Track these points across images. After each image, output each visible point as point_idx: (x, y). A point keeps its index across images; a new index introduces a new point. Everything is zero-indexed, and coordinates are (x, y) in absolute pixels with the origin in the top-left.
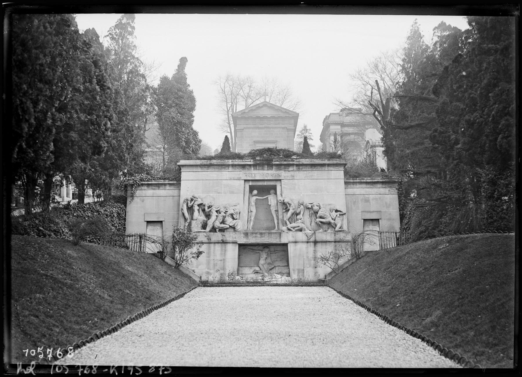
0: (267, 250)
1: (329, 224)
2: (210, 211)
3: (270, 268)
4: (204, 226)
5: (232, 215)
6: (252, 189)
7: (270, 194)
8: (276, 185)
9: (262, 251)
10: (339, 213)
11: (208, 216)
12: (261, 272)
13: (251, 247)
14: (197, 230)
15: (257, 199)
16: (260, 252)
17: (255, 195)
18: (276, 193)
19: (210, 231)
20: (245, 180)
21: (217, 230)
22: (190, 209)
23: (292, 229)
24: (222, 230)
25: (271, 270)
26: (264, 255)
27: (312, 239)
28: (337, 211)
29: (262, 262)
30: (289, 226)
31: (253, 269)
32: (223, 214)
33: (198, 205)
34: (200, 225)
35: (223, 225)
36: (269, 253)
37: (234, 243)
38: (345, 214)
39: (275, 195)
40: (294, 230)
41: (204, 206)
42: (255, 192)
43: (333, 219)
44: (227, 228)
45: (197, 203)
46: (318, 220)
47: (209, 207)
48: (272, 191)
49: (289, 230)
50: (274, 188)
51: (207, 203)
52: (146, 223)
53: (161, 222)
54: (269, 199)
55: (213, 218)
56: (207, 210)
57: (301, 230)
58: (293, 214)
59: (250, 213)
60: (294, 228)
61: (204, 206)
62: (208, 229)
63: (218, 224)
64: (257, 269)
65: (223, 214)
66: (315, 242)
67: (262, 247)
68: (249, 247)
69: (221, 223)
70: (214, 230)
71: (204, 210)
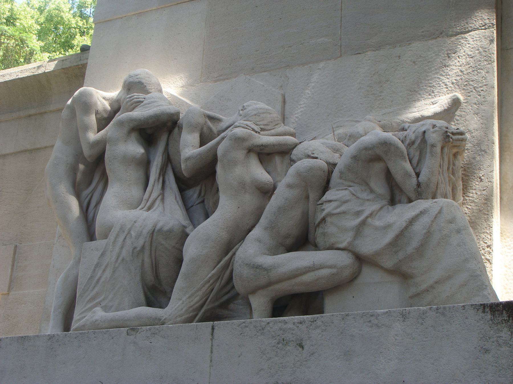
24: (300, 301)
44: (341, 284)
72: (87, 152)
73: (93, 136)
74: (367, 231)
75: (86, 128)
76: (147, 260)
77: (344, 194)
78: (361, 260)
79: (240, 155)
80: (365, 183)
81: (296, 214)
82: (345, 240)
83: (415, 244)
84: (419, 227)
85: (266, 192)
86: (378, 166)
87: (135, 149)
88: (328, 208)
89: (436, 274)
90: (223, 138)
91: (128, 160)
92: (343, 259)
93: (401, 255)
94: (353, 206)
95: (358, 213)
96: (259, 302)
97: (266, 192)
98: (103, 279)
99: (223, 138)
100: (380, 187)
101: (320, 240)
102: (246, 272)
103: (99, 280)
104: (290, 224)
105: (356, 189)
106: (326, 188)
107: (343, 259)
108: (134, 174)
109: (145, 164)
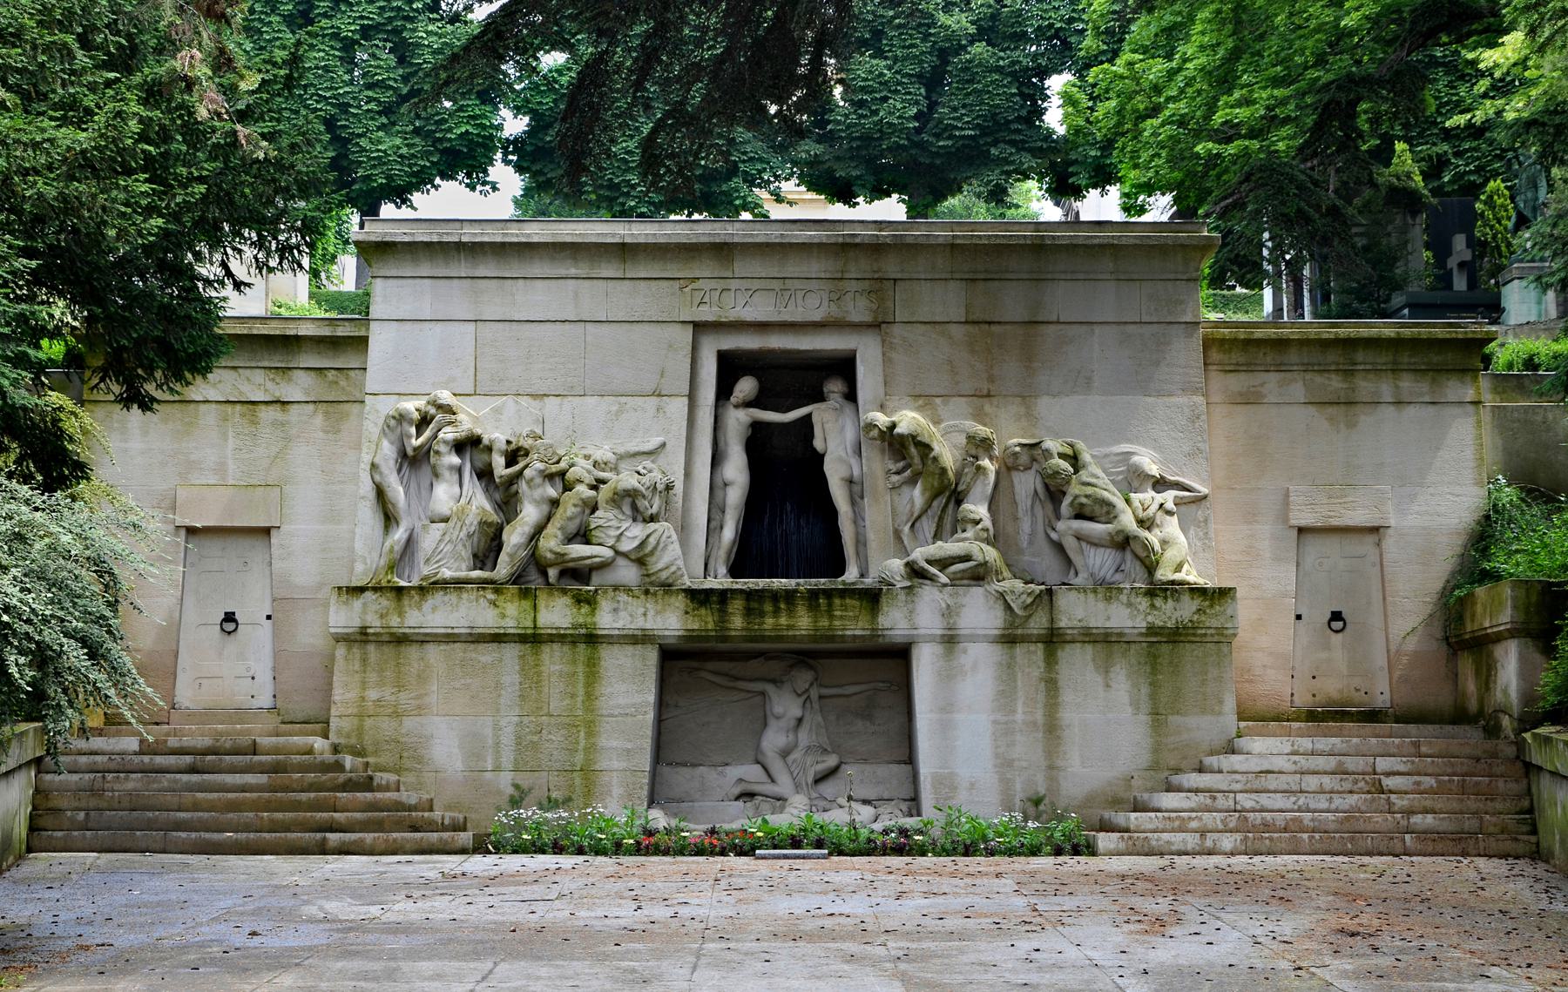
0: (803, 678)
1: (1123, 542)
2: (520, 474)
3: (820, 767)
4: (488, 547)
5: (631, 495)
6: (730, 367)
7: (819, 397)
9: (774, 681)
10: (1169, 497)
11: (507, 500)
12: (769, 788)
13: (726, 666)
14: (447, 573)
15: (756, 426)
16: (770, 688)
17: (748, 404)
18: (851, 396)
19: (517, 578)
20: (699, 327)
21: (553, 573)
22: (414, 461)
23: (933, 570)
24: (577, 574)
25: (817, 781)
26: (786, 705)
27: (1038, 624)
28: (1160, 484)
29: (774, 739)
30: (919, 554)
31: (734, 772)
32: (582, 490)
33: (459, 447)
34: (466, 554)
35: (578, 550)
36: (814, 693)
37: (640, 639)
38: (1205, 497)
40: (944, 579)
41: (489, 449)
42: (746, 387)
43: (1141, 522)
44: (604, 565)
45: (448, 434)
46: (1067, 527)
47: (513, 457)
48: (835, 387)
49: (916, 573)
50: (844, 367)
51: (497, 435)
52: (183, 533)
53: (266, 531)
54: (815, 419)
55: (530, 513)
56: (500, 468)
57: (979, 575)
59: (719, 493)
60: (943, 563)
61: (489, 449)
62: (503, 569)
63: (550, 543)
64: (752, 772)
65: (582, 490)
66: (1053, 640)
68: (711, 665)
69: (570, 540)
70: (536, 572)
71: (485, 474)
72: (410, 452)
73: (416, 442)
75: (410, 437)
77: (610, 515)
78: (617, 553)
79: (538, 480)
80: (619, 508)
81: (577, 521)
82: (611, 542)
83: (649, 548)
84: (652, 540)
85: (555, 503)
86: (628, 500)
87: (455, 460)
88: (601, 522)
89: (660, 565)
91: (451, 468)
92: (609, 553)
94: (614, 523)
96: (553, 573)
97: (555, 503)
100: (627, 509)
101: (594, 540)
102: (549, 555)
104: (573, 527)
105: (616, 512)
106: (594, 509)
107: (609, 553)
109: (460, 470)
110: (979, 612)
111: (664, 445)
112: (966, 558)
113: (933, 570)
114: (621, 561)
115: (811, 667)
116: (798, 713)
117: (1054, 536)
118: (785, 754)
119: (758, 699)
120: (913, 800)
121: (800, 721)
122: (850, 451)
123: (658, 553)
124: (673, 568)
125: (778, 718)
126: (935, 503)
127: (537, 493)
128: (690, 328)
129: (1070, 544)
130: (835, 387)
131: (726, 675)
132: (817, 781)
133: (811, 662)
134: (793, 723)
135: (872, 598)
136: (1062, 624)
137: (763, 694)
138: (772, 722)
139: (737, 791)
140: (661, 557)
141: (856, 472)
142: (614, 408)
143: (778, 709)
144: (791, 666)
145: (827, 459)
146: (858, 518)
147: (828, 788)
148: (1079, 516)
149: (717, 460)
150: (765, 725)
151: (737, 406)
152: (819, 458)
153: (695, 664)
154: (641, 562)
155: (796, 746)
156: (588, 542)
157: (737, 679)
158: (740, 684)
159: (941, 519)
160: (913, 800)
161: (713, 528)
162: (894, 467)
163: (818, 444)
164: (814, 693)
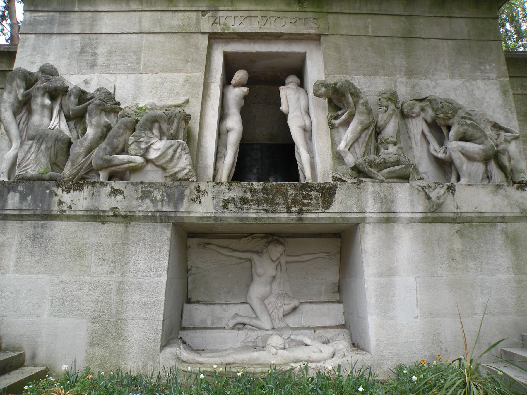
0: (276, 251)
3: (288, 308)
8: (305, 54)
9: (257, 252)
16: (255, 257)
18: (302, 85)
25: (284, 316)
26: (265, 267)
29: (257, 290)
31: (233, 309)
39: (302, 91)
42: (240, 75)
46: (454, 145)
48: (292, 79)
58: (365, 129)
59: (223, 137)
67: (264, 241)
74: (151, 150)
76: (52, 152)
87: (48, 102)
90: (90, 104)
92: (139, 160)
93: (163, 161)
95: (147, 143)
98: (31, 158)
99: (90, 104)
103: (29, 158)
108: (47, 112)
110: (406, 200)
111: (188, 101)
112: (397, 163)
113: (374, 171)
114: (149, 167)
115: (281, 243)
116: (273, 273)
117: (441, 155)
118: (263, 300)
119: (248, 263)
120: (343, 326)
121: (274, 278)
122: (303, 112)
123: (175, 161)
124: (186, 171)
125: (259, 276)
126: (363, 135)
127: (94, 120)
128: (207, 37)
129: (458, 158)
130: (292, 79)
131: (227, 248)
132: (284, 316)
133: (281, 239)
134: (270, 279)
135: (327, 193)
136: (464, 210)
137: (250, 260)
138: (256, 278)
139: (234, 322)
140: (177, 164)
141: (307, 123)
142: (158, 81)
143: (260, 271)
144: (269, 243)
145: (289, 117)
146: (310, 152)
147: (293, 321)
148: (461, 140)
149: (222, 116)
150: (251, 280)
151: (235, 86)
152: (284, 116)
153: (206, 240)
154: (164, 169)
155: (271, 293)
156: (127, 153)
157: (234, 250)
158: (236, 254)
159: (367, 144)
160: (343, 326)
161: (219, 156)
162: (334, 114)
163: (283, 108)
164: (283, 260)
